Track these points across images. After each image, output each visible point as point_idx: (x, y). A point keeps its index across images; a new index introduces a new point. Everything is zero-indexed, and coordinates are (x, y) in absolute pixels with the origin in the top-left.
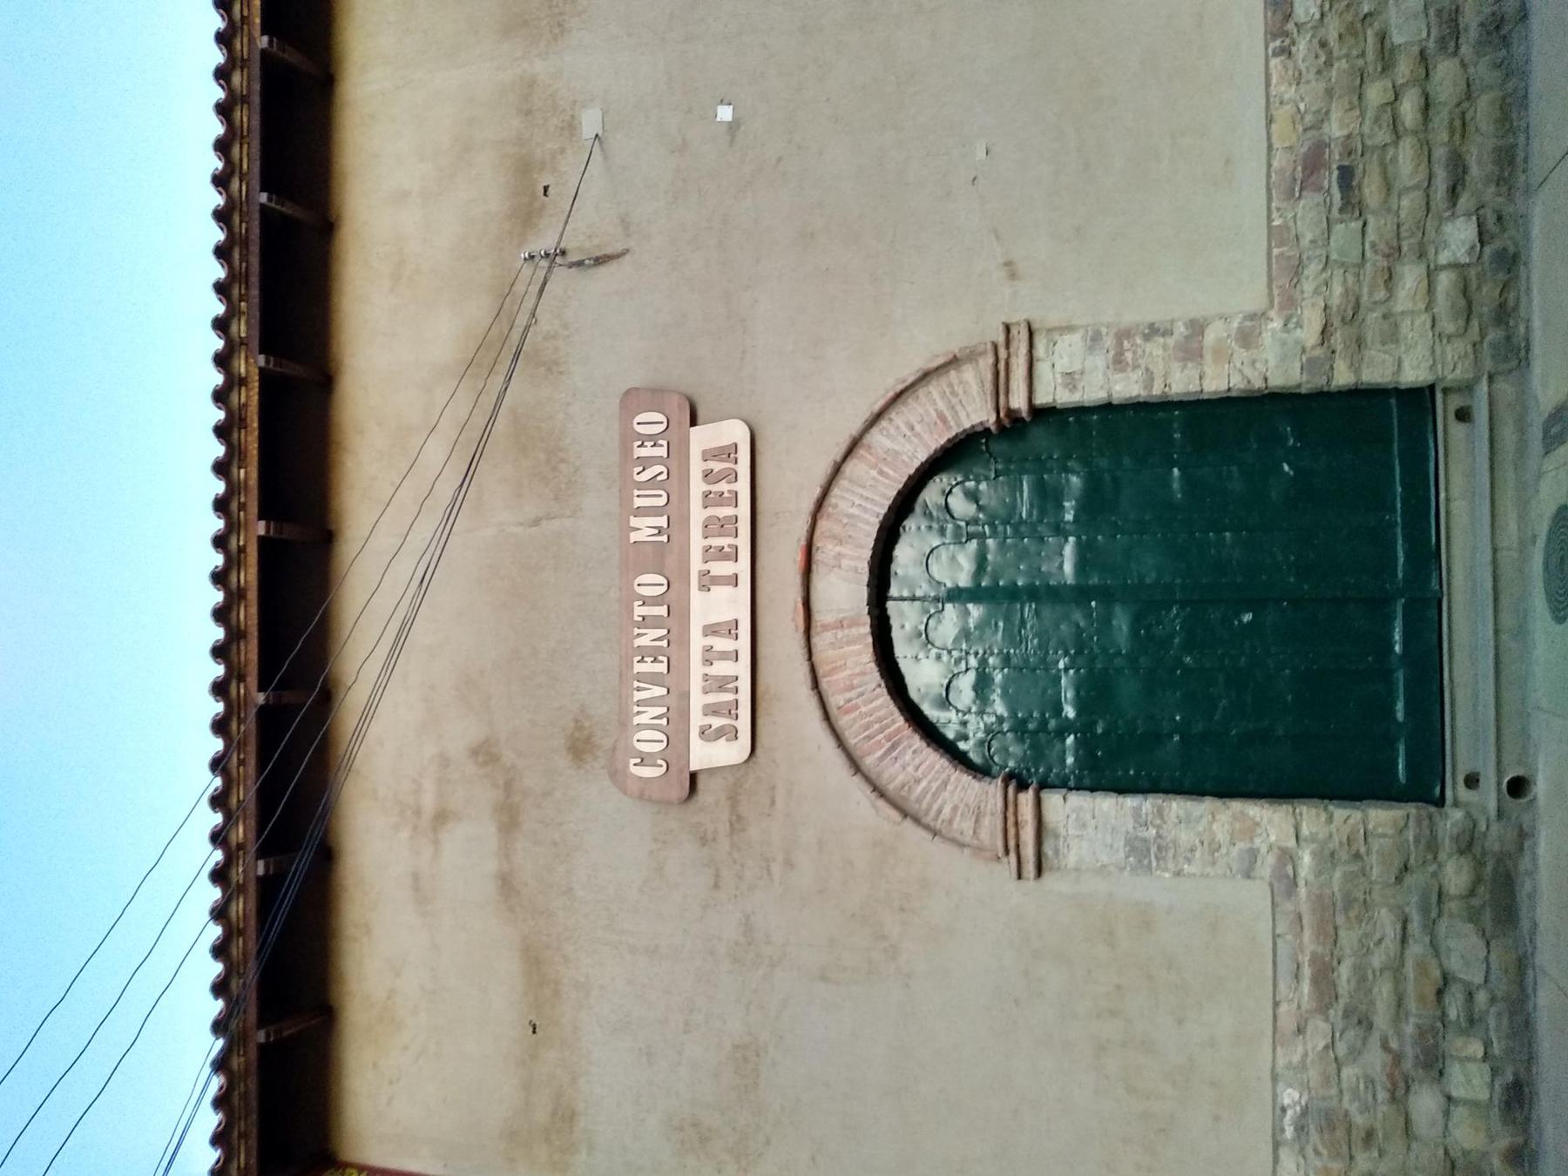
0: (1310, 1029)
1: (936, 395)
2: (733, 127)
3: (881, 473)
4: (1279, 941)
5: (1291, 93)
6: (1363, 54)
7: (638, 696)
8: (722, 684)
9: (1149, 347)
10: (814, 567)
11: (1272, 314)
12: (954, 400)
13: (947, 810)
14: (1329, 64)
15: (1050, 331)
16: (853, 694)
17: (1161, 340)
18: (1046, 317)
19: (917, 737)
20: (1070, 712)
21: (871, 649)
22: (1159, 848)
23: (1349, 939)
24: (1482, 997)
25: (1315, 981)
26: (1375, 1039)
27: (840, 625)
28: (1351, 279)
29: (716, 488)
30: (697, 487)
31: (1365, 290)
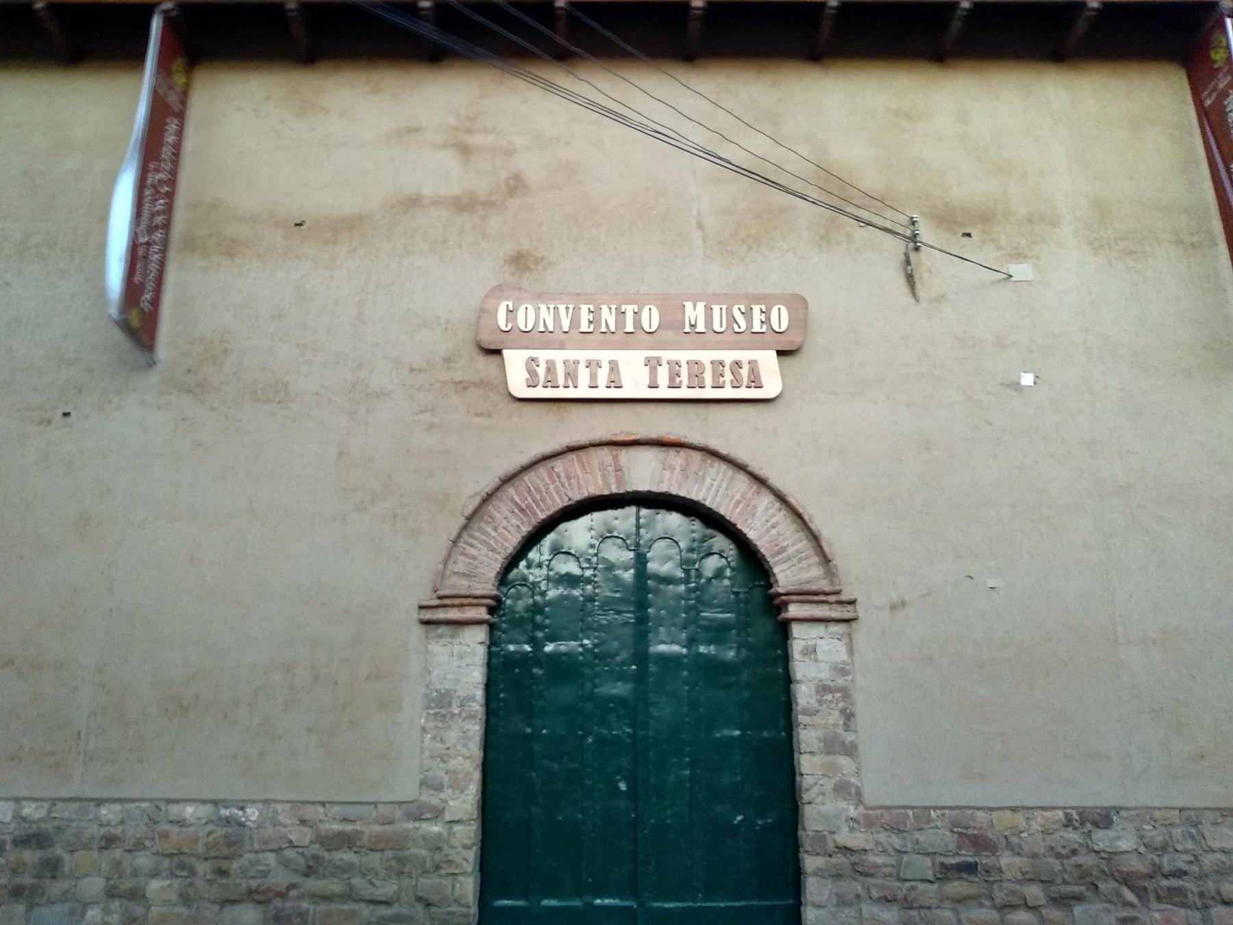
0: (305, 829)
1: (799, 546)
2: (1017, 386)
3: (738, 502)
4: (372, 807)
5: (1036, 826)
6: (1065, 882)
7: (562, 308)
8: (571, 375)
9: (837, 713)
10: (664, 449)
11: (861, 809)
12: (795, 560)
13: (473, 551)
14: (1058, 856)
15: (850, 635)
16: (564, 479)
17: (841, 723)
18: (861, 633)
19: (530, 529)
20: (549, 648)
21: (598, 493)
22: (444, 716)
23: (374, 859)
25: (341, 834)
26: (296, 879)
27: (618, 469)
30: (728, 356)
31: (880, 881)
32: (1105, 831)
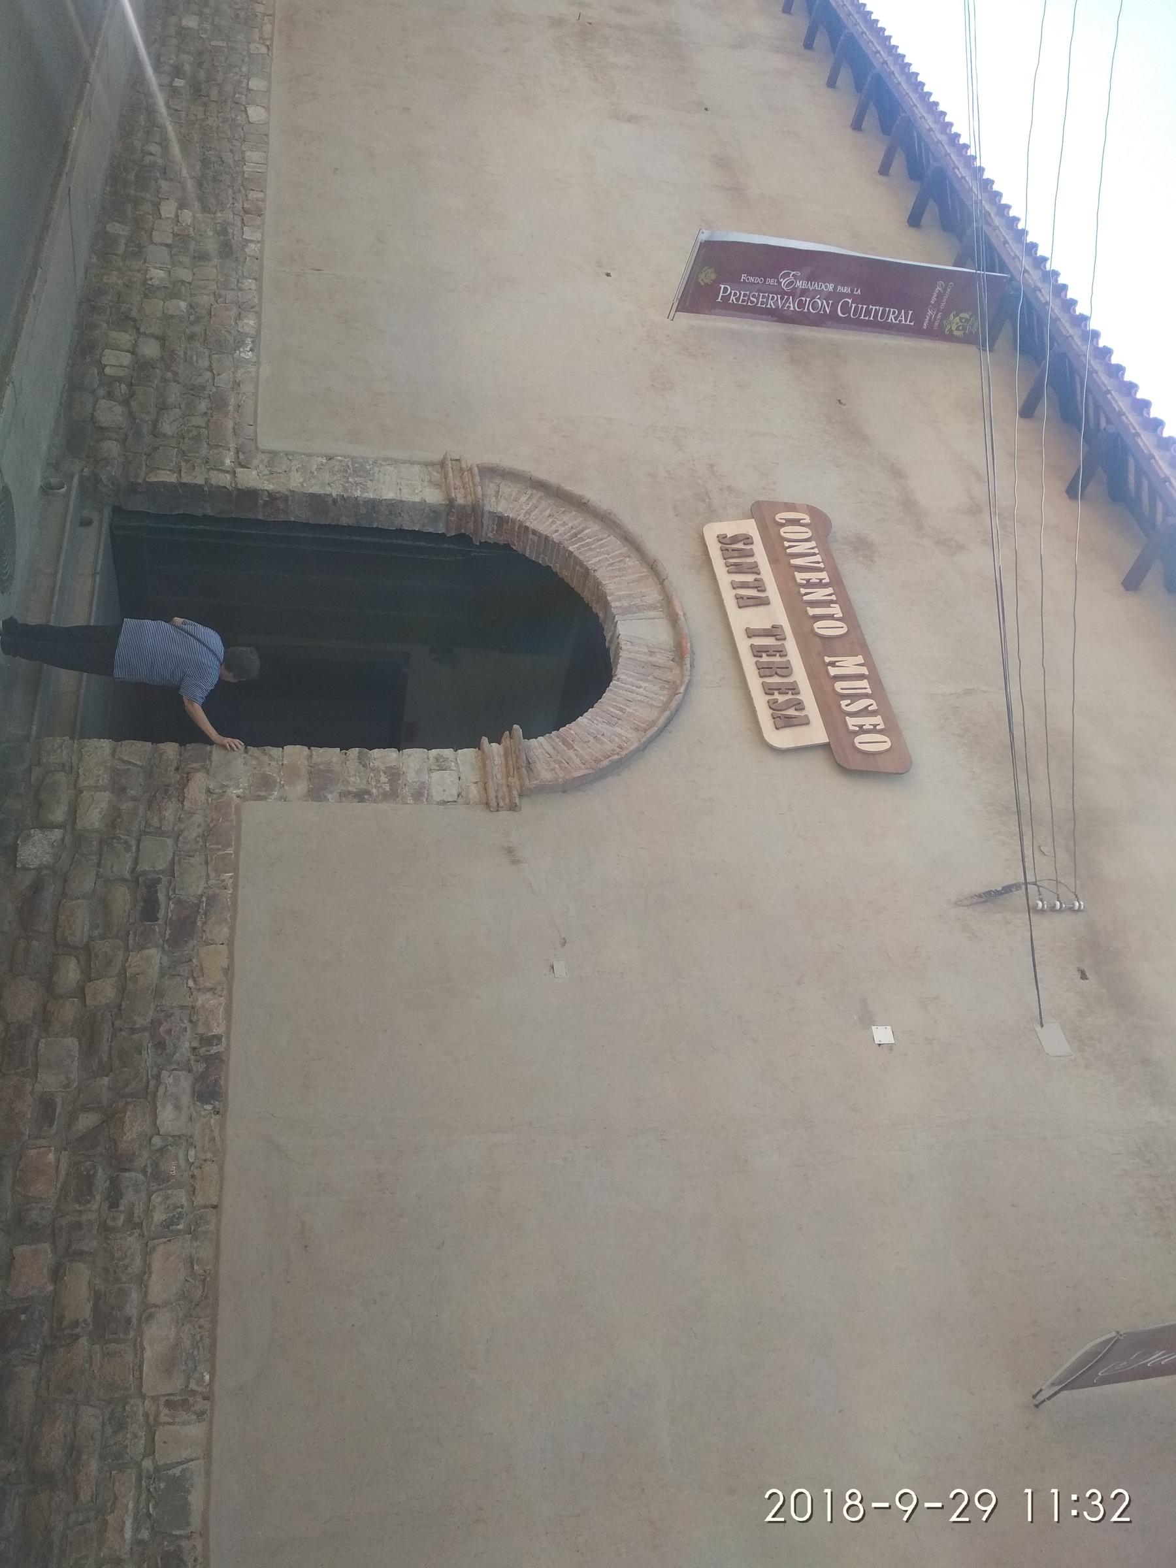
2: (868, 1020)
3: (621, 710)
5: (202, 999)
6: (114, 1036)
7: (818, 558)
11: (238, 800)
14: (155, 1024)
17: (350, 788)
24: (101, 392)
28: (155, 822)
29: (789, 696)
30: (807, 695)
31: (141, 811)
32: (188, 1090)
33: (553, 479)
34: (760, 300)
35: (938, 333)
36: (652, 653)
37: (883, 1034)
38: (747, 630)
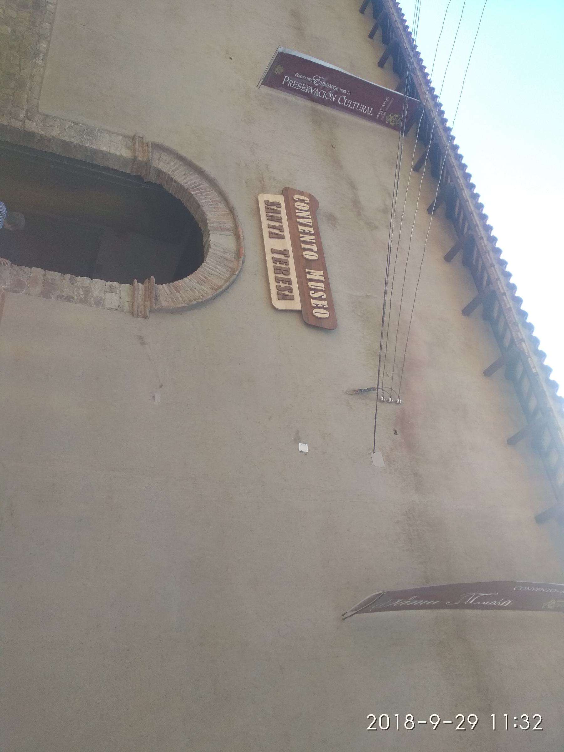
2: (298, 440)
3: (206, 278)
7: (310, 221)
11: (4, 291)
17: (63, 294)
22: (83, 132)
29: (287, 285)
30: (295, 286)
33: (189, 156)
34: (302, 87)
35: (383, 122)
36: (225, 252)
37: (303, 447)
38: (272, 249)
